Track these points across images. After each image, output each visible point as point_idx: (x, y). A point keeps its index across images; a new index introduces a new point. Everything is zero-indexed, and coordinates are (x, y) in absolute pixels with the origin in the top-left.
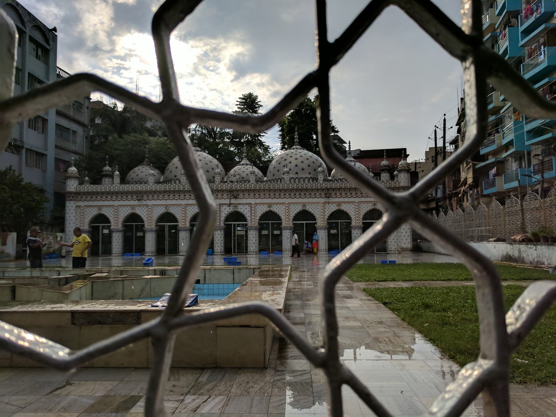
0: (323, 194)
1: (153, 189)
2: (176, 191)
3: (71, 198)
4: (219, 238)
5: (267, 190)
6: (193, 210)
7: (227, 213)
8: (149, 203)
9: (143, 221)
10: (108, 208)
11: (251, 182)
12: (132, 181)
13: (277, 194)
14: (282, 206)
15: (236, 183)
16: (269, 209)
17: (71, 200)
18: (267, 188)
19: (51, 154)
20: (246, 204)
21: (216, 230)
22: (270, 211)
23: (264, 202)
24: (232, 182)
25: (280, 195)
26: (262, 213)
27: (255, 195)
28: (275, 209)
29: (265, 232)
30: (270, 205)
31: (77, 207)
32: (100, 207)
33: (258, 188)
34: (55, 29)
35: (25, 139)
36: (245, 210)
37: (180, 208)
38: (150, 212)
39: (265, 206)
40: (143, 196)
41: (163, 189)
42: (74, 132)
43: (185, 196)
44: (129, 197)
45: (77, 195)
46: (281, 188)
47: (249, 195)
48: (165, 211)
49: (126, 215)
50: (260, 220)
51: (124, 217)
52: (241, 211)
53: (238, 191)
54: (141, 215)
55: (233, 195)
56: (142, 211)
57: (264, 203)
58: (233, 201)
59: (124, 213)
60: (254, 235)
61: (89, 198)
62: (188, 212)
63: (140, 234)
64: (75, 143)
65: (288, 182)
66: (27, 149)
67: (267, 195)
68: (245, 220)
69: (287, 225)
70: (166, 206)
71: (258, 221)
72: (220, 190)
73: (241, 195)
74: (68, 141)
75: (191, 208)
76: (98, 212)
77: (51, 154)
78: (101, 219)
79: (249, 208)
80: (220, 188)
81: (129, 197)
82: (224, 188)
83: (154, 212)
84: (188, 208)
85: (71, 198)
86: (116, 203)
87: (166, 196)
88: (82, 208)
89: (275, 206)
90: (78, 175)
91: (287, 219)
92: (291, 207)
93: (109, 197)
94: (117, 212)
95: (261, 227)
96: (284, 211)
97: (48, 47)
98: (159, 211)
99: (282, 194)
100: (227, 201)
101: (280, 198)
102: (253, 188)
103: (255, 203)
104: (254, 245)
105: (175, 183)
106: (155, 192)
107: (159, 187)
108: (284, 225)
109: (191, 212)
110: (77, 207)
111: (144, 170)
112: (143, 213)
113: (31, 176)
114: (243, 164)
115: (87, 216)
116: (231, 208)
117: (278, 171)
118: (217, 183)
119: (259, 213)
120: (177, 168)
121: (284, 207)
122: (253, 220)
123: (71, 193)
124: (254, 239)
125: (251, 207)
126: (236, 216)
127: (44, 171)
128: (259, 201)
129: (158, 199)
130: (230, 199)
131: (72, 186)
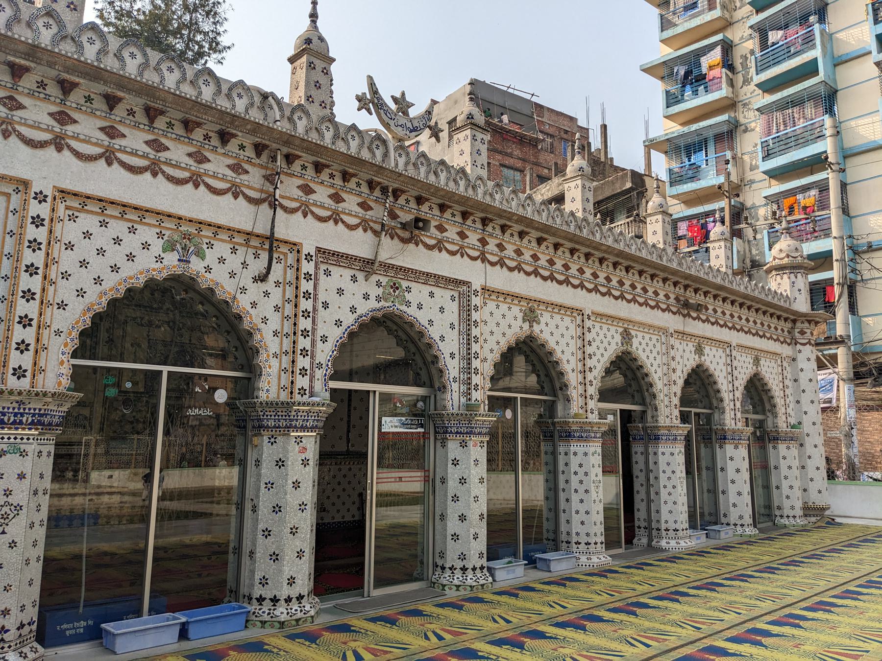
0: (672, 296)
6: (116, 255)
7: (349, 320)
23: (516, 289)
27: (483, 242)
36: (437, 317)
39: (516, 310)
52: (421, 317)
57: (514, 296)
67: (527, 256)
75: (102, 237)
79: (455, 306)
84: (70, 231)
96: (573, 348)
100: (359, 244)
109: (99, 266)
121: (573, 331)
125: (466, 310)
126: (393, 349)
128: (499, 278)
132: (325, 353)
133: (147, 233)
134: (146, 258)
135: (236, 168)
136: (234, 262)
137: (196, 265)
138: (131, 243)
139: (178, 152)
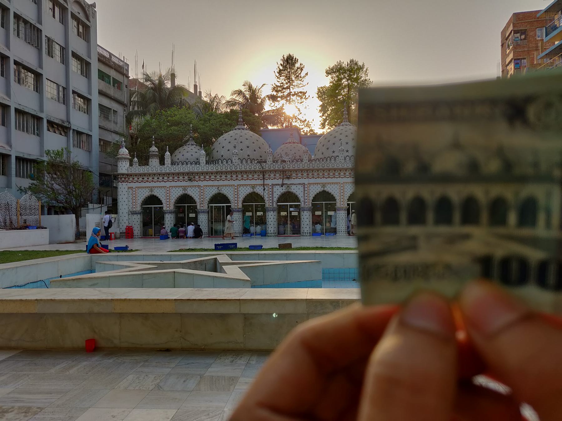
1: (205, 170)
2: (228, 171)
3: (123, 179)
4: (272, 219)
5: (321, 169)
6: (245, 191)
7: (279, 194)
8: (201, 183)
9: (195, 203)
10: (159, 189)
11: (304, 162)
12: (178, 161)
13: (331, 174)
14: (336, 185)
15: (289, 163)
16: (322, 189)
17: (123, 181)
18: (321, 167)
19: (96, 134)
20: (300, 184)
21: (268, 211)
22: (324, 191)
23: (318, 182)
24: (285, 161)
25: (334, 174)
26: (315, 193)
27: (308, 175)
28: (328, 189)
29: (318, 213)
30: (324, 185)
31: (129, 188)
32: (151, 189)
33: (311, 168)
34: (94, 5)
35: (71, 121)
37: (232, 189)
38: (202, 193)
40: (194, 177)
41: (215, 170)
42: (115, 112)
43: (237, 176)
44: (181, 178)
45: (127, 177)
46: (335, 167)
47: (302, 175)
48: (217, 192)
49: (177, 196)
50: (313, 201)
51: (176, 198)
52: (294, 191)
53: (291, 171)
54: (193, 196)
55: (286, 175)
56: (194, 192)
57: (317, 183)
58: (286, 181)
59: (176, 193)
60: (308, 216)
61: (141, 179)
62: (240, 193)
63: (192, 215)
64: (116, 123)
65: (343, 161)
66: (73, 130)
67: (321, 174)
68: (299, 201)
69: (342, 206)
70: (218, 187)
71: (311, 201)
72: (272, 170)
73: (294, 175)
74: (110, 121)
75: (243, 189)
76: (150, 193)
77: (96, 134)
78: (153, 200)
80: (272, 169)
81: (181, 178)
82: (277, 168)
83: (206, 193)
84: (240, 189)
85: (123, 179)
86: (168, 184)
87: (218, 177)
88: (134, 190)
89: (329, 185)
90: (129, 157)
91: (342, 200)
92: (346, 187)
93: (161, 178)
94: (169, 194)
95: (314, 208)
97: (88, 23)
98: (211, 192)
99: (337, 174)
100: (280, 182)
101: (334, 177)
102: (306, 167)
103: (309, 184)
104: (308, 227)
105: (222, 163)
106: (207, 173)
107: (211, 168)
108: (338, 205)
110: (129, 188)
111: (189, 149)
112: (195, 194)
113: (78, 157)
114: (290, 143)
115: (138, 198)
116: (284, 188)
117: (328, 149)
118: (269, 163)
119: (312, 193)
120: (223, 147)
121: (338, 187)
122: (306, 200)
123: (123, 175)
124: (308, 220)
125: (304, 188)
127: (89, 151)
128: (312, 181)
129: (210, 180)
130: (283, 179)
131: (123, 167)
132: (275, 199)
133: (248, 187)
134: (249, 190)
135: (259, 176)
136: (260, 188)
137: (255, 190)
138: (247, 189)
139: (250, 176)
